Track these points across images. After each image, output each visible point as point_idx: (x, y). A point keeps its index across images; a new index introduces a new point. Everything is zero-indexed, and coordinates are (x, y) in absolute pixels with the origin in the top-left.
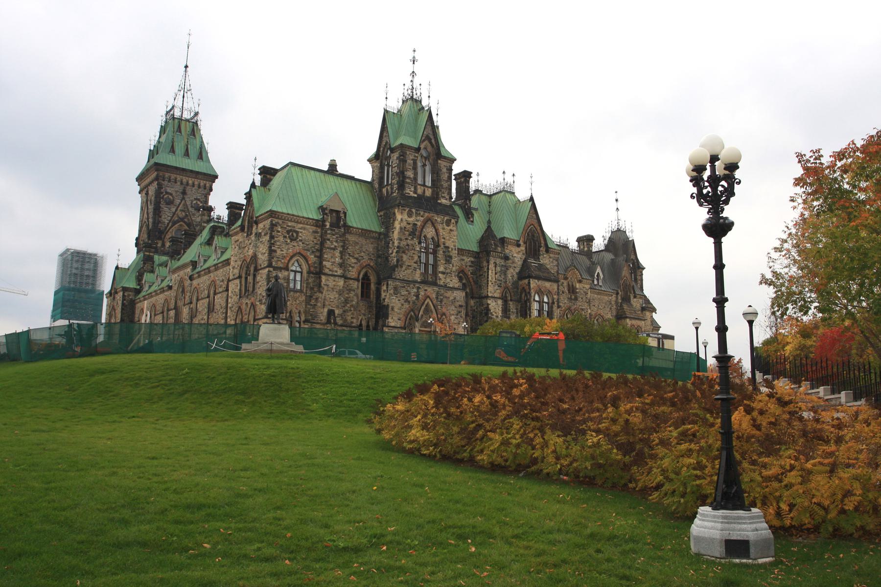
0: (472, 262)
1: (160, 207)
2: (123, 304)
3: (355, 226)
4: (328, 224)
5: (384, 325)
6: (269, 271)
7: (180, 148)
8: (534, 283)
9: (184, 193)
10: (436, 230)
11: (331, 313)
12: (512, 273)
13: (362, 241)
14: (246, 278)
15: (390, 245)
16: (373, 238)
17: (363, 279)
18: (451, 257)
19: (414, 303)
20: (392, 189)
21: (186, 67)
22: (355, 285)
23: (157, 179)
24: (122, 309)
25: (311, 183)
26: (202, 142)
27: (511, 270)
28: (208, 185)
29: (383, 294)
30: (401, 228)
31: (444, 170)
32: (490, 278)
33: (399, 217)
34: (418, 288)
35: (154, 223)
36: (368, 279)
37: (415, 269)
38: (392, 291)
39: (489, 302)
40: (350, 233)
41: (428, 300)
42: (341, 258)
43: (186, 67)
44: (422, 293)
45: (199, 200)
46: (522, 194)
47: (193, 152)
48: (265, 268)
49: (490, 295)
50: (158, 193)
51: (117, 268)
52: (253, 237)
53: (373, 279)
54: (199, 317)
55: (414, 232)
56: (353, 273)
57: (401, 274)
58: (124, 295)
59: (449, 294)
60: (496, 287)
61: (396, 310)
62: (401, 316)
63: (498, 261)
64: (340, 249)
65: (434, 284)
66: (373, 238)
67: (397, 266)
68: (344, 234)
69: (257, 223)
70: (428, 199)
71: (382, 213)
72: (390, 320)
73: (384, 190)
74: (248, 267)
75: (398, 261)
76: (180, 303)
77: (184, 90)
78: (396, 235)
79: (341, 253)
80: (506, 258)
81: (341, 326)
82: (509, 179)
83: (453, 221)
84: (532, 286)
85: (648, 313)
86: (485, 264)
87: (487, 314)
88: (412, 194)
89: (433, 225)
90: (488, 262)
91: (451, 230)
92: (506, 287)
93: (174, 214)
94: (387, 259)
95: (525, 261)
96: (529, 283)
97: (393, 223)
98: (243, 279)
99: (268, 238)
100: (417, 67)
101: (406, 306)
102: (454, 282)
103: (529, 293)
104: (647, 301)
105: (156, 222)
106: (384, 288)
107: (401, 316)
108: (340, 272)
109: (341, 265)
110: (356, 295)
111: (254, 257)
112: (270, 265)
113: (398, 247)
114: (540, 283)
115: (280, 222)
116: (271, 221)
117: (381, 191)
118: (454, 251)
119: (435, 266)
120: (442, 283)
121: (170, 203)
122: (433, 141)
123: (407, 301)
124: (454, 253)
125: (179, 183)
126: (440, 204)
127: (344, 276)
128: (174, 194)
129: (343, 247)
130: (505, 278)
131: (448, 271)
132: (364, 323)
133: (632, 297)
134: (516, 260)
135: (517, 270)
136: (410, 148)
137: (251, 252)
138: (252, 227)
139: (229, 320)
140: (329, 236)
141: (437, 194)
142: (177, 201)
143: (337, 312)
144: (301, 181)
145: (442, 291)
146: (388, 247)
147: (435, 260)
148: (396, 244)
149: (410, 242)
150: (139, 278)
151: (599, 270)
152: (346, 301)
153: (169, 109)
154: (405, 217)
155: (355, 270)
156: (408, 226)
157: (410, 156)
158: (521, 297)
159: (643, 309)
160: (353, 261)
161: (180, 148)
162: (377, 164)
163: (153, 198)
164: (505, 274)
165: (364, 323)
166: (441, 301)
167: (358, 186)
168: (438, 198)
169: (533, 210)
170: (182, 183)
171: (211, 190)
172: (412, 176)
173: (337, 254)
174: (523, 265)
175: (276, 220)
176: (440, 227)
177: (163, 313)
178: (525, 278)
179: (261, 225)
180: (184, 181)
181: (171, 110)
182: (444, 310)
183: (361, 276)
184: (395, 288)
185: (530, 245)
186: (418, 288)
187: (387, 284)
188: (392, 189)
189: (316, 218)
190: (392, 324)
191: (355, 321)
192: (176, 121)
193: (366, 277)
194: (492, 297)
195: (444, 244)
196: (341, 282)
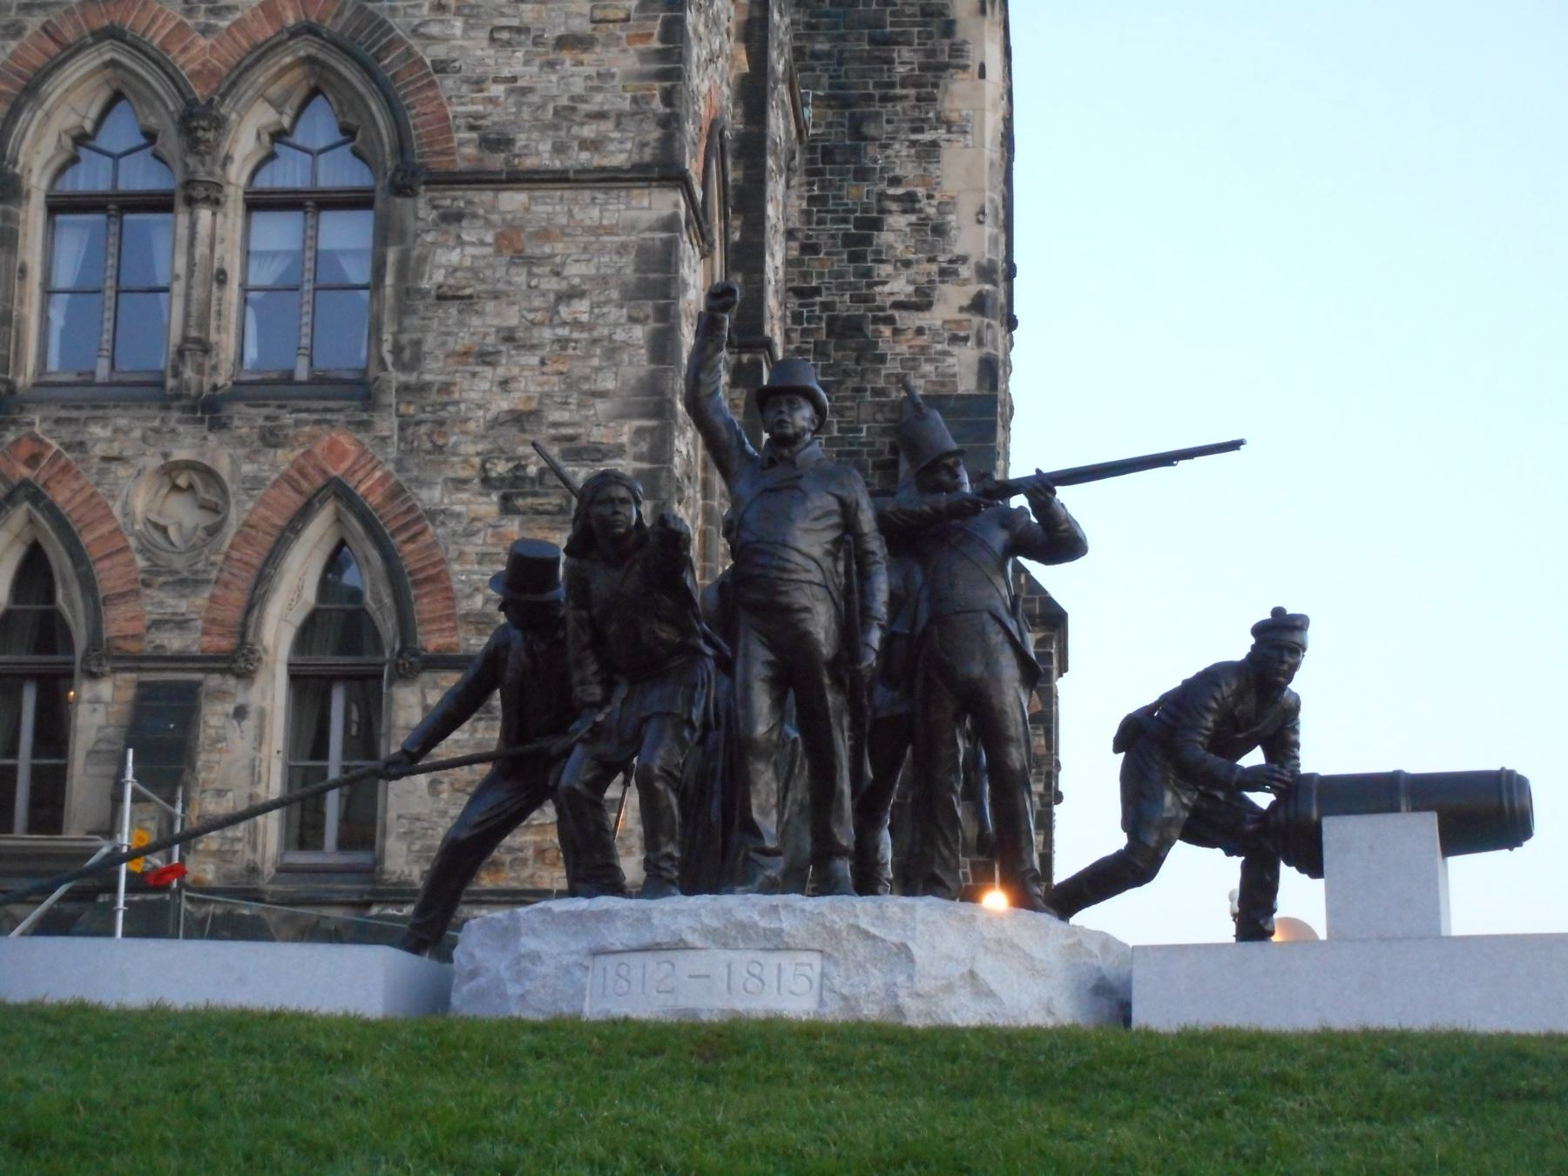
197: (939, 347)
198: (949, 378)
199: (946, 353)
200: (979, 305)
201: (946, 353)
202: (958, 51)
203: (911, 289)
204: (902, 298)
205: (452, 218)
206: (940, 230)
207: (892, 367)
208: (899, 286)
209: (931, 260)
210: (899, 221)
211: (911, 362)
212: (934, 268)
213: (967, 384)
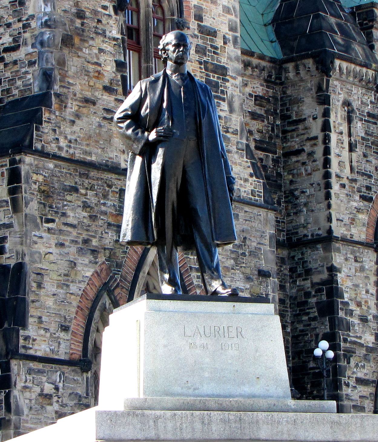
38: (33, 208)
61: (50, 287)
72: (32, 330)
75: (47, 77)
190: (41, 348)
195: (199, 18)
197: (23, 70)
198: (28, 87)
199: (27, 73)
201: (27, 73)
203: (11, 39)
204: (7, 45)
209: (19, 21)
211: (12, 81)
212: (21, 25)
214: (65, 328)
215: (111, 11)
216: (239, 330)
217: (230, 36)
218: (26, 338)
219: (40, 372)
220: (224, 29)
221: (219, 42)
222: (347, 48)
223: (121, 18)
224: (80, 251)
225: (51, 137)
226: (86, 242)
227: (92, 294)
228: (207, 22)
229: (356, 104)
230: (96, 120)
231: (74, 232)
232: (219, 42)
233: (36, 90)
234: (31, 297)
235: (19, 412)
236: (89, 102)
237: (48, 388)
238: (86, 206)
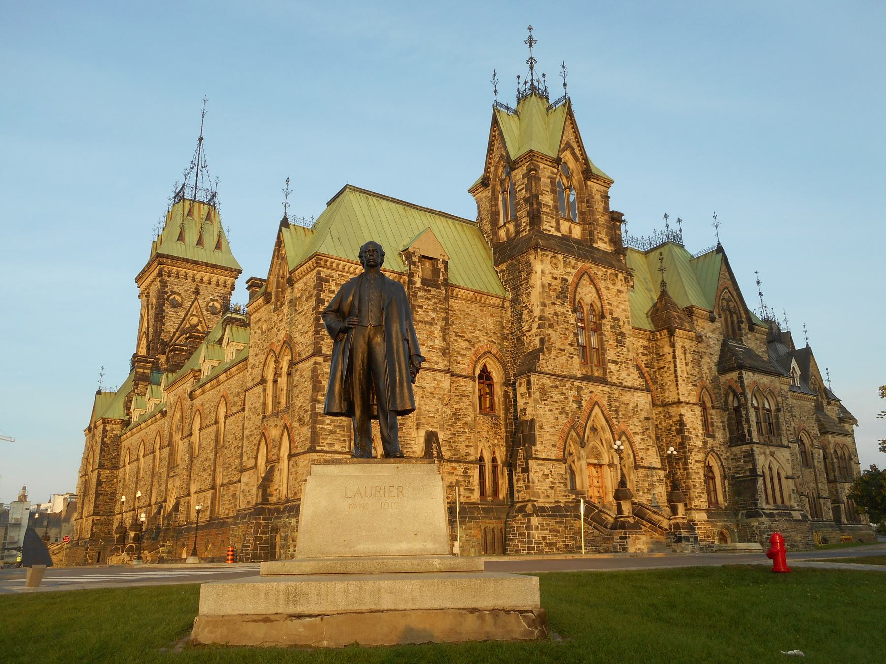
0: (645, 348)
1: (164, 311)
2: (103, 443)
3: (462, 285)
4: (418, 281)
5: (528, 457)
6: (316, 363)
7: (191, 237)
8: (749, 377)
9: (197, 292)
10: (598, 291)
11: (431, 438)
12: (709, 363)
13: (474, 309)
14: (275, 381)
15: (525, 317)
16: (494, 306)
17: (480, 377)
18: (623, 335)
19: (575, 413)
20: (518, 225)
21: (201, 139)
22: (471, 387)
23: (160, 274)
24: (102, 450)
25: (384, 219)
26: (221, 228)
27: (706, 360)
28: (229, 282)
29: (521, 402)
30: (543, 286)
31: (597, 197)
32: (679, 373)
33: (538, 266)
34: (579, 388)
35: (155, 332)
36: (489, 378)
37: (571, 356)
38: (537, 395)
39: (683, 410)
40: (456, 297)
41: (596, 409)
42: (444, 340)
43: (201, 139)
44: (586, 397)
45: (217, 301)
46: (697, 244)
47: (210, 241)
48: (308, 358)
49: (682, 400)
50: (162, 295)
51: (99, 392)
52: (286, 309)
53: (497, 375)
54: (203, 456)
55: (565, 293)
56: (464, 366)
57: (550, 363)
58: (105, 430)
59: (627, 397)
60: (690, 387)
61: (547, 429)
62: (555, 438)
63: (687, 344)
64: (441, 323)
65: (603, 381)
66: (494, 306)
67: (541, 350)
68: (447, 298)
69: (291, 282)
70: (576, 241)
71: (504, 266)
72: (538, 446)
73: (502, 233)
74: (277, 362)
75: (542, 341)
76: (177, 437)
77: (198, 167)
78: (535, 297)
79: (444, 331)
80: (699, 339)
81: (451, 461)
82: (675, 227)
83: (620, 276)
84: (746, 382)
85: (847, 426)
86: (667, 349)
87: (680, 431)
88: (553, 232)
89: (592, 281)
90: (673, 345)
91: (619, 291)
92: (704, 387)
93: (184, 319)
94: (519, 339)
95: (724, 344)
96: (741, 377)
97: (527, 280)
98: (270, 385)
99: (312, 303)
100: (536, 52)
101: (563, 419)
102: (632, 378)
103: (743, 394)
104: (843, 409)
105: (158, 332)
106: (522, 389)
107: (555, 438)
108: (442, 364)
109: (445, 352)
110: (472, 405)
111: (289, 342)
112: (317, 352)
113: (541, 318)
114: (757, 377)
115: (335, 274)
116: (319, 274)
117: (495, 233)
118: (626, 325)
119: (601, 350)
120: (614, 380)
121: (176, 305)
122: (577, 150)
123: (563, 411)
124: (626, 329)
125: (190, 280)
126: (597, 249)
127: (448, 371)
128: (183, 293)
129: (446, 319)
130: (700, 372)
131: (622, 359)
132: (487, 457)
133: (825, 404)
134: (712, 342)
135: (716, 358)
136: (545, 158)
137: (282, 335)
138: (283, 291)
139: (245, 458)
140: (420, 301)
141: (591, 234)
142: (187, 304)
143: (441, 436)
144: (367, 213)
145: (616, 392)
146: (520, 319)
147: (601, 342)
148: (537, 312)
149: (559, 309)
150: (127, 407)
151: (794, 364)
152: (456, 415)
153: (178, 190)
154: (548, 267)
155: (467, 360)
156: (554, 283)
157: (546, 172)
158: (726, 402)
159: (841, 420)
160: (465, 345)
161: (191, 237)
162: (487, 193)
163: (154, 301)
164: (700, 366)
165: (487, 457)
166: (616, 411)
167: (459, 227)
168: (592, 241)
169: (724, 267)
170: (194, 280)
171: (233, 288)
172: (551, 203)
173: (437, 332)
174: (722, 351)
175: (327, 271)
176: (602, 285)
177: (153, 452)
178: (732, 370)
179: (299, 285)
180: (198, 277)
181: (180, 192)
182: (623, 428)
183: (478, 372)
184: (543, 389)
185: (726, 320)
186: (579, 388)
187: (529, 383)
188: (518, 225)
189: (397, 269)
191: (471, 451)
192: (187, 203)
193: (485, 376)
194: (686, 403)
195: (611, 314)
196: (446, 382)
200: (539, 327)
202: (532, 269)
205: (296, 370)
206: (531, 312)
207: (526, 346)
208: (526, 327)
210: (525, 312)
211: (529, 344)
213: (538, 346)
214: (554, 446)
215: (570, 312)
216: (400, 489)
217: (626, 320)
218: (536, 451)
219: (542, 465)
220: (623, 318)
221: (621, 323)
222: (682, 324)
223: (575, 315)
224: (561, 413)
225: (545, 365)
226: (562, 408)
227: (566, 431)
228: (615, 315)
229: (687, 347)
230: (565, 358)
231: (557, 405)
232: (621, 323)
233: (538, 346)
234: (537, 433)
235: (533, 482)
236: (561, 350)
237: (547, 472)
238: (562, 393)
